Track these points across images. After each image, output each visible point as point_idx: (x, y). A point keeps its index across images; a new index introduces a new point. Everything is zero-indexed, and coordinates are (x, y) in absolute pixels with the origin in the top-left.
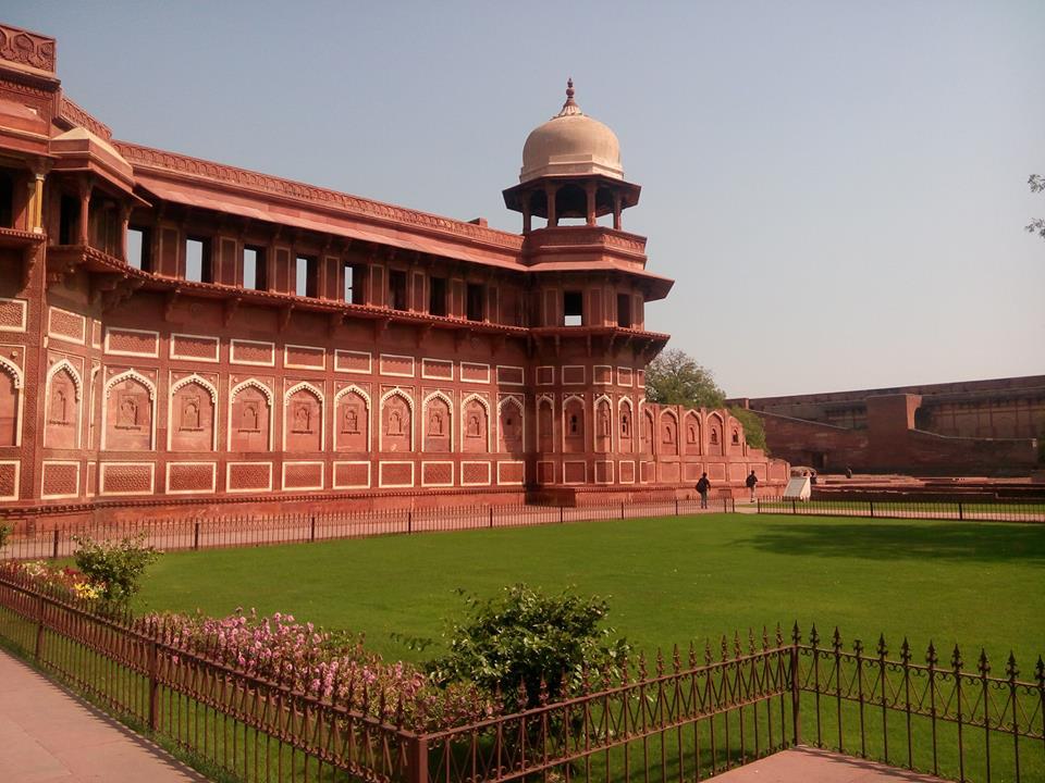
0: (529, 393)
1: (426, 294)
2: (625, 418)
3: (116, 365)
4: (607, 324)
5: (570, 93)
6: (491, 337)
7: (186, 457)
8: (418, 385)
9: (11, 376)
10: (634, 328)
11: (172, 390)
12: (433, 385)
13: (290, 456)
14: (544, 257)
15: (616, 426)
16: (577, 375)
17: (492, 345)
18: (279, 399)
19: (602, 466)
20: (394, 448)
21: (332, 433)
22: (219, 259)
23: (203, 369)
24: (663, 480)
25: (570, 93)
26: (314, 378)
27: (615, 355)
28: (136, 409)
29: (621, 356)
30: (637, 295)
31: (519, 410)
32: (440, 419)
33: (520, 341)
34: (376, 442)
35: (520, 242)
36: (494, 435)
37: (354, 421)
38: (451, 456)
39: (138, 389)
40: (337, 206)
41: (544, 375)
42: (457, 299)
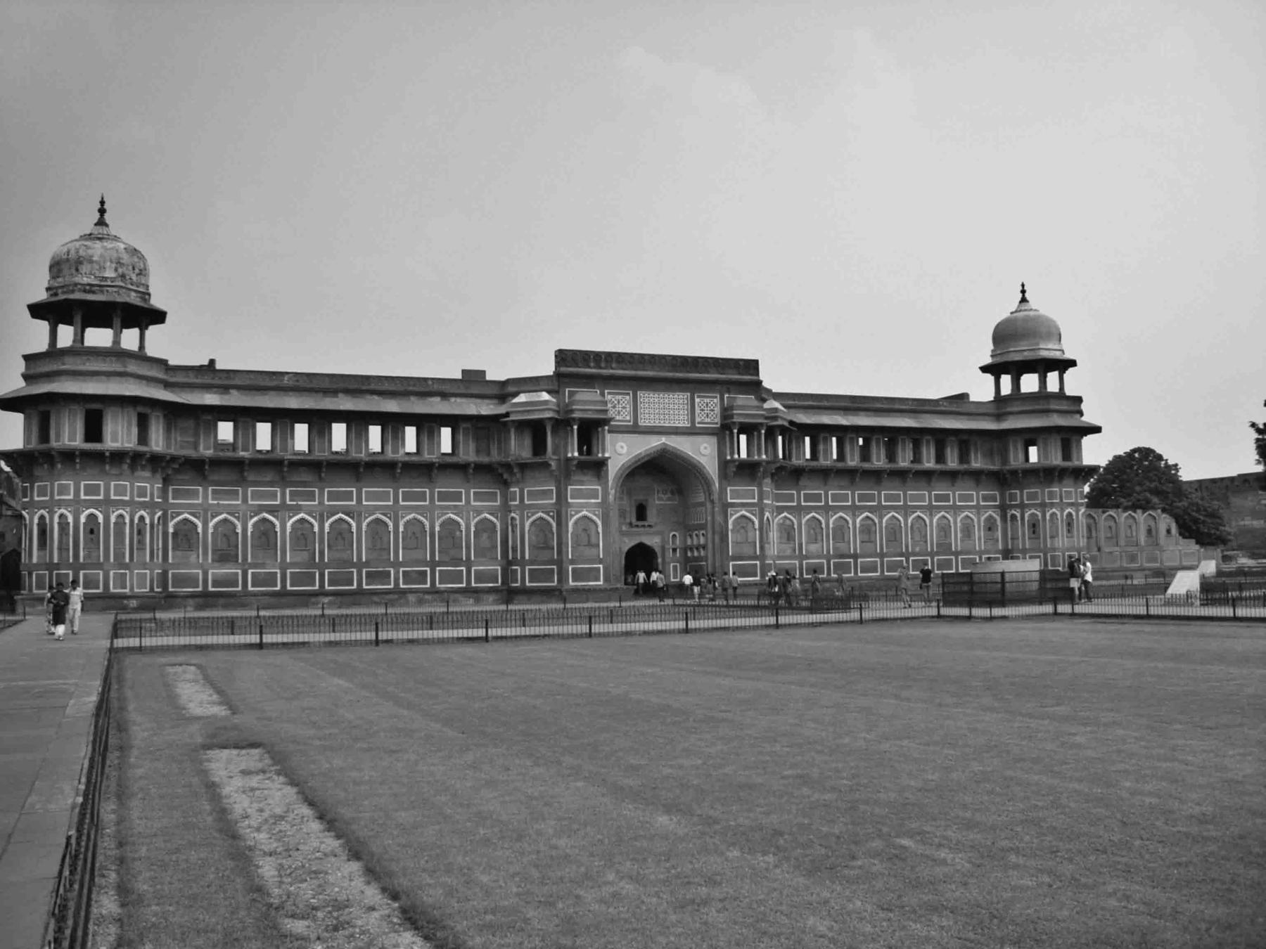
0: (1003, 509)
1: (933, 451)
2: (1069, 525)
3: (780, 510)
5: (1023, 292)
6: (977, 476)
8: (931, 509)
9: (753, 523)
10: (1076, 463)
11: (804, 521)
12: (940, 508)
14: (1011, 417)
15: (1062, 529)
18: (854, 523)
19: (1053, 557)
20: (917, 549)
21: (880, 541)
22: (821, 447)
24: (1105, 565)
25: (1023, 292)
26: (870, 509)
28: (788, 533)
29: (1065, 482)
30: (1074, 438)
32: (944, 529)
34: (907, 547)
35: (992, 405)
37: (894, 533)
38: (952, 554)
40: (879, 405)
41: (1012, 497)
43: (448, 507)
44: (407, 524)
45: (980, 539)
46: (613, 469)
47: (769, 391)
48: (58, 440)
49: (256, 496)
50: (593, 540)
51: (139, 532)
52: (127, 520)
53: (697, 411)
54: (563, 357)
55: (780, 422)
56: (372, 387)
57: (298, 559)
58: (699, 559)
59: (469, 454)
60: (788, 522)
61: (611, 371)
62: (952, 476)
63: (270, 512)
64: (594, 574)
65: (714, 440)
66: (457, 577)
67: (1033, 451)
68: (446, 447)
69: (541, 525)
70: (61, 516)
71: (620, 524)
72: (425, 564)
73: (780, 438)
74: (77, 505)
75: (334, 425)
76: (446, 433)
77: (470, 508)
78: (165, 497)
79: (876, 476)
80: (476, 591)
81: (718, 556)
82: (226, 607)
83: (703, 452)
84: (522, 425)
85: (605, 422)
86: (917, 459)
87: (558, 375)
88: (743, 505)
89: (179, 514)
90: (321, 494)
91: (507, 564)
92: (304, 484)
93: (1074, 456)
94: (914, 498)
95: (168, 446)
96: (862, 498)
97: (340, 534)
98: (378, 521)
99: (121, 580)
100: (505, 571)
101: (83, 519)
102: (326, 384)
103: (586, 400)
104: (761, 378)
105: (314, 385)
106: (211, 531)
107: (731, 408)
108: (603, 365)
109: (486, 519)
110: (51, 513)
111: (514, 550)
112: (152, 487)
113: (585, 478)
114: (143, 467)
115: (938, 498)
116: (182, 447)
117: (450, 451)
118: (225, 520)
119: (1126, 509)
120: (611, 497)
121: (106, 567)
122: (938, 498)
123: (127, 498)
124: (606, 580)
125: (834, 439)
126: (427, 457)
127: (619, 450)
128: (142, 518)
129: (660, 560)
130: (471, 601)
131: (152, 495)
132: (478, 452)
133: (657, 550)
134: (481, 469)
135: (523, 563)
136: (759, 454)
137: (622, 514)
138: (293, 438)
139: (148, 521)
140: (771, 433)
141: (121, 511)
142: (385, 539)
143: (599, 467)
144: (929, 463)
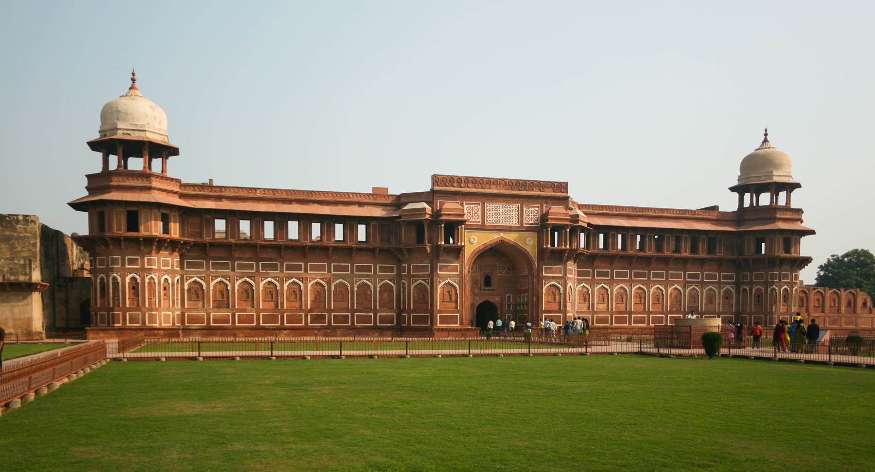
0: (737, 285)
1: (689, 245)
3: (579, 282)
4: (777, 254)
7: (601, 313)
9: (559, 289)
10: (794, 255)
13: (635, 313)
16: (761, 277)
17: (720, 263)
18: (630, 292)
22: (610, 241)
23: (605, 281)
26: (643, 283)
27: (780, 267)
28: (586, 297)
29: (784, 267)
31: (732, 292)
32: (694, 297)
33: (734, 261)
36: (719, 304)
39: (585, 290)
41: (745, 277)
42: (703, 245)
43: (363, 276)
44: (336, 286)
45: (719, 304)
46: (468, 252)
47: (574, 203)
48: (110, 229)
49: (241, 267)
50: (453, 298)
51: (165, 289)
52: (156, 281)
53: (525, 215)
54: (436, 179)
55: (580, 223)
56: (314, 198)
57: (268, 307)
58: (524, 312)
59: (377, 243)
60: (585, 290)
61: (467, 190)
62: (702, 262)
63: (248, 277)
64: (453, 320)
65: (535, 234)
66: (368, 319)
67: (763, 244)
68: (362, 235)
69: (420, 288)
70: (115, 278)
71: (472, 291)
72: (347, 310)
73: (582, 235)
74: (124, 272)
75: (289, 222)
76: (362, 229)
77: (376, 278)
78: (182, 267)
79: (647, 262)
80: (380, 328)
81: (535, 310)
82: (221, 335)
83: (529, 244)
84: (409, 223)
85: (462, 222)
86: (677, 250)
87: (433, 191)
88: (553, 277)
89: (191, 278)
90: (282, 267)
91: (400, 311)
92: (271, 260)
93: (793, 250)
94: (673, 276)
95: (182, 234)
96: (636, 275)
97: (294, 291)
98: (318, 283)
99: (152, 319)
100: (398, 316)
101: (128, 280)
102: (284, 196)
103: (450, 207)
104: (569, 194)
105: (277, 196)
106: (211, 288)
107: (547, 214)
108: (462, 185)
109: (387, 283)
110: (108, 276)
111: (404, 304)
112: (173, 260)
113: (449, 258)
114: (166, 249)
115: (690, 276)
116: (192, 236)
117: (364, 240)
118: (221, 282)
119: (831, 288)
120: (466, 271)
121: (143, 309)
122: (690, 276)
123: (156, 267)
124: (461, 323)
125: (620, 236)
126: (349, 244)
127: (472, 240)
128: (166, 280)
129: (499, 312)
130: (377, 334)
131: (173, 266)
132: (382, 240)
133: (497, 305)
134: (382, 250)
135: (409, 312)
136: (565, 245)
137: (474, 282)
138: (263, 230)
139: (170, 282)
140: (575, 231)
141: (153, 276)
142: (322, 295)
143: (457, 252)
144: (686, 254)
